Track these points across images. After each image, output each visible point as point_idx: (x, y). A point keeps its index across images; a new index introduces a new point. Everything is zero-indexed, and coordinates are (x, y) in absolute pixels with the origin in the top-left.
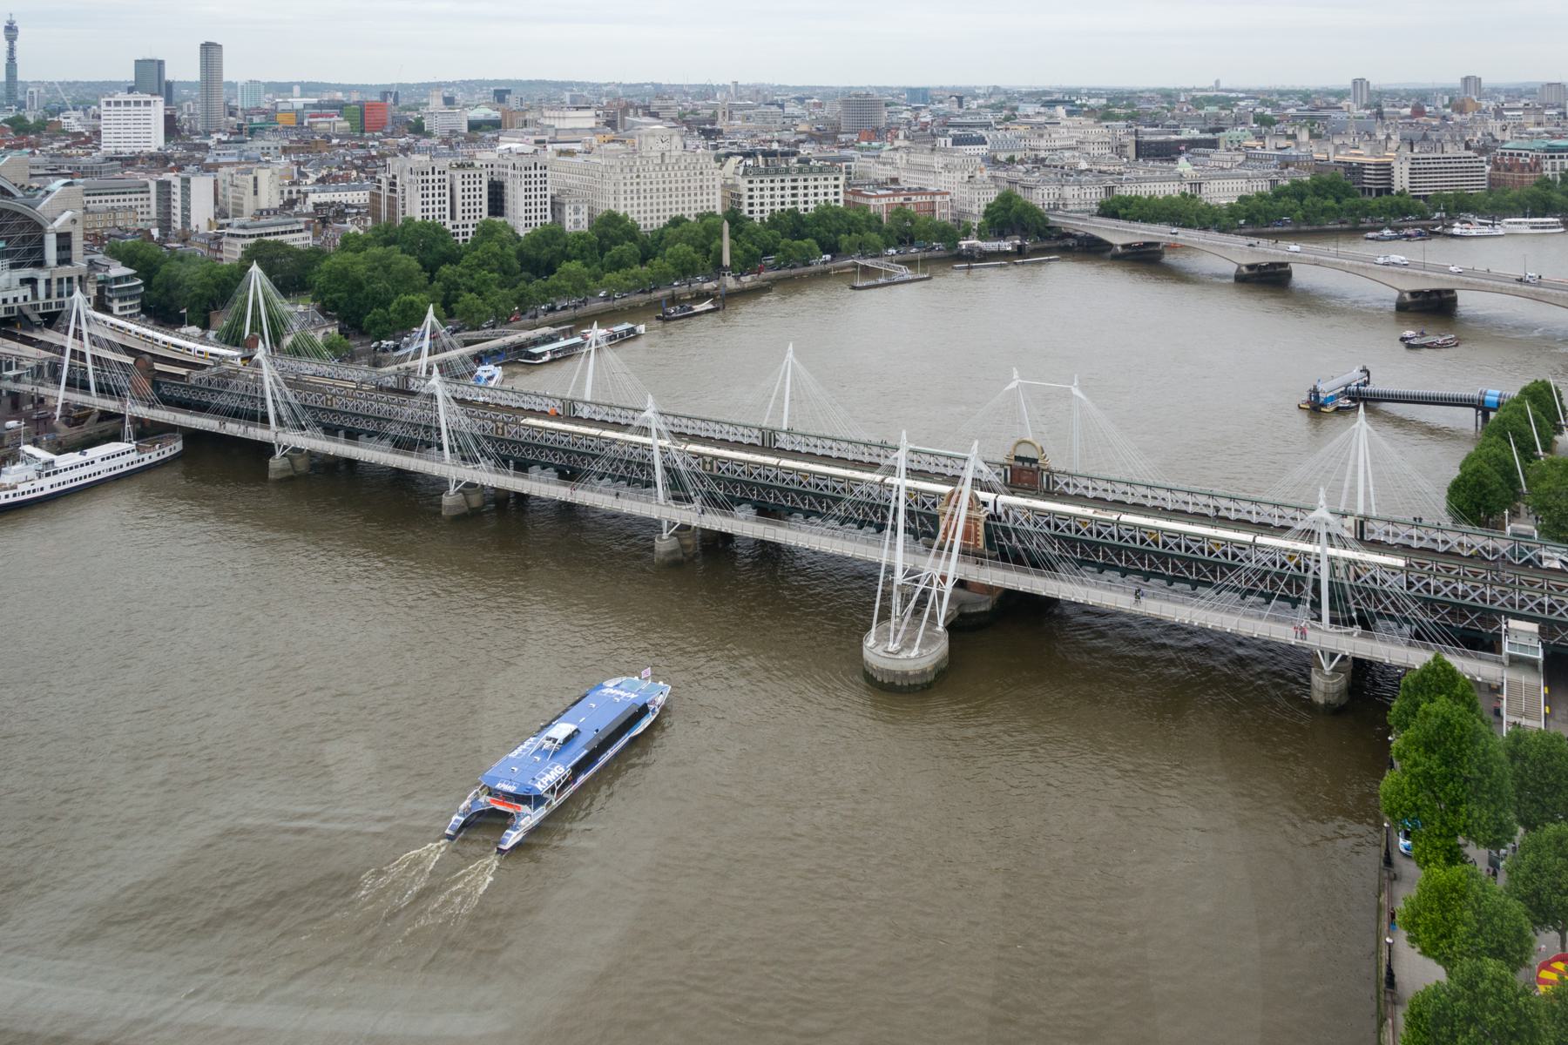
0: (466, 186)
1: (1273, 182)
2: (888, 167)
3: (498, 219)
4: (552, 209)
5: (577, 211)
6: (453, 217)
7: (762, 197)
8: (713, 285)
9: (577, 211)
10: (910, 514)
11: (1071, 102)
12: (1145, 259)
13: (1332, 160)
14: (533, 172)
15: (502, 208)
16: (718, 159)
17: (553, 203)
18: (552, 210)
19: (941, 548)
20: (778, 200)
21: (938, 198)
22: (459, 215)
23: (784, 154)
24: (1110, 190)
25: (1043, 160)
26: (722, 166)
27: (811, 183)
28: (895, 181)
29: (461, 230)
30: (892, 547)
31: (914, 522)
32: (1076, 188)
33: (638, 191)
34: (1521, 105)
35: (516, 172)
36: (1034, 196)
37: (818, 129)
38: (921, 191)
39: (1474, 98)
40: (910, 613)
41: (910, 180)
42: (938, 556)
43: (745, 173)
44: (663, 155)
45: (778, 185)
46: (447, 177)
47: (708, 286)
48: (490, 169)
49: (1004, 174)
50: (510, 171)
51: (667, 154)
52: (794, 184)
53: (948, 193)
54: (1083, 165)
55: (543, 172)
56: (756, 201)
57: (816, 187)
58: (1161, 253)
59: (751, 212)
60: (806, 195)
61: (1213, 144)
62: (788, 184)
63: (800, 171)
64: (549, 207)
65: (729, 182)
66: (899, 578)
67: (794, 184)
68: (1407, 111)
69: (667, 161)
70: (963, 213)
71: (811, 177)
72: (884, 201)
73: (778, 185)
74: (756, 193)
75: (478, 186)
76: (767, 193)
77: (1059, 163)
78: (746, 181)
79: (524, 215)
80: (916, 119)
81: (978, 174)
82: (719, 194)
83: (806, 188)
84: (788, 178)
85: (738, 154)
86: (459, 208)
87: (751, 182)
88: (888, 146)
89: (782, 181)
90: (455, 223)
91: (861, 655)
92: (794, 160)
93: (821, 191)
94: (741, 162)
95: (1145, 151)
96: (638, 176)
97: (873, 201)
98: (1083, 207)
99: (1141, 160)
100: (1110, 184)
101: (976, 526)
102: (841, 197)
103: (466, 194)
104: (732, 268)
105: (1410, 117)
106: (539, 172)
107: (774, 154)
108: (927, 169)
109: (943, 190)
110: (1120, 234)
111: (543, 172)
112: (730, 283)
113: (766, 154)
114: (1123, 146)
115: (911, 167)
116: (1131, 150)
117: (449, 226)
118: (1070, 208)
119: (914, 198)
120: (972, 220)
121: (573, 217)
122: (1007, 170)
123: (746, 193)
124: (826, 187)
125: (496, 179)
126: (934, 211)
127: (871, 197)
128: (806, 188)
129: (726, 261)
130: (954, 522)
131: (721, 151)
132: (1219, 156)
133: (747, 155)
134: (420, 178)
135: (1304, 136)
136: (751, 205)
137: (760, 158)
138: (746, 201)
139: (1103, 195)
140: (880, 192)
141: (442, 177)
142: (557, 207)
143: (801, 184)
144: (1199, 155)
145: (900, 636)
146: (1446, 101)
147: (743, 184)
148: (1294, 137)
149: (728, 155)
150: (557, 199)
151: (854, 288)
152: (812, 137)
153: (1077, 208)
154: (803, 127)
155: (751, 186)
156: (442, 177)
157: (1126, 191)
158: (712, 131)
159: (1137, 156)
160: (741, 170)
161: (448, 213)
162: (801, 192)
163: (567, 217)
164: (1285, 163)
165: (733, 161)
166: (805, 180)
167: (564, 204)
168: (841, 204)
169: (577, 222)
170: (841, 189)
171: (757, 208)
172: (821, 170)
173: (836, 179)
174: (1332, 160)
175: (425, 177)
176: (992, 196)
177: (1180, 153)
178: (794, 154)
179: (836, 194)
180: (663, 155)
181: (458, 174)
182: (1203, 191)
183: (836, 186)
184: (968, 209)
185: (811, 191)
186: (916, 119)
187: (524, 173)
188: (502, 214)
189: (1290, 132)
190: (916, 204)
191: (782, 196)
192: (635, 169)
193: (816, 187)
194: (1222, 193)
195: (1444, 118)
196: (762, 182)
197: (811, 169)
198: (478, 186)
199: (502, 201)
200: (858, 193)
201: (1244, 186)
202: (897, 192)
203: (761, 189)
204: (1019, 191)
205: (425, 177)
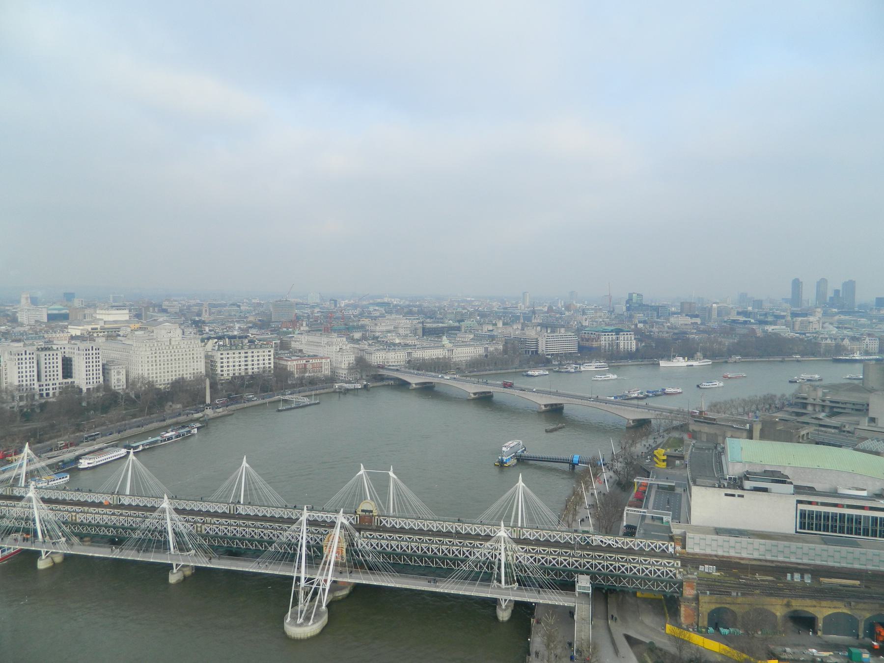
0: (48, 361)
1: (486, 349)
2: (297, 343)
3: (69, 380)
4: (103, 372)
5: (119, 373)
6: (39, 380)
7: (228, 362)
8: (200, 415)
9: (119, 373)
10: (309, 547)
11: (390, 309)
12: (427, 390)
13: (512, 337)
14: (91, 352)
15: (71, 373)
16: (202, 341)
17: (103, 369)
18: (103, 373)
19: (325, 564)
20: (237, 364)
21: (324, 361)
22: (43, 378)
23: (240, 337)
24: (409, 354)
25: (377, 338)
26: (206, 344)
27: (255, 354)
28: (301, 351)
29: (44, 387)
30: (299, 568)
31: (310, 551)
32: (393, 353)
33: (156, 361)
34: (593, 307)
35: (80, 352)
36: (373, 358)
37: (260, 320)
38: (315, 357)
39: (574, 302)
40: (308, 601)
41: (308, 350)
42: (323, 569)
43: (219, 350)
44: (170, 340)
45: (237, 355)
46: (34, 356)
47: (196, 416)
48: (63, 350)
49: (357, 346)
50: (76, 352)
51: (173, 339)
52: (246, 355)
54: (397, 341)
55: (97, 352)
56: (225, 364)
57: (258, 356)
58: (434, 387)
59: (222, 371)
60: (253, 361)
61: (458, 329)
62: (243, 355)
63: (250, 348)
64: (101, 372)
65: (210, 353)
66: (303, 583)
67: (246, 355)
68: (546, 309)
69: (173, 343)
70: (336, 368)
71: (255, 351)
72: (295, 363)
73: (237, 355)
74: (225, 360)
75: (55, 361)
76: (231, 360)
77: (385, 340)
78: (219, 353)
79: (85, 377)
80: (312, 314)
81: (344, 347)
82: (203, 361)
83: (253, 357)
84: (242, 351)
85: (215, 338)
86: (43, 374)
87: (222, 354)
88: (297, 332)
89: (240, 353)
90: (41, 383)
91: (283, 628)
92: (246, 341)
93: (261, 358)
94: (216, 343)
95: (427, 332)
96: (155, 353)
97: (289, 363)
98: (396, 364)
99: (425, 337)
100: (410, 351)
101: (342, 551)
102: (272, 361)
103: (48, 365)
105: (547, 312)
106: (94, 352)
107: (234, 337)
108: (318, 345)
109: (326, 355)
111: (97, 352)
112: (209, 412)
113: (230, 338)
114: (416, 329)
115: (309, 343)
116: (420, 332)
117: (36, 386)
118: (391, 364)
119: (311, 361)
120: (341, 371)
121: (116, 377)
122: (359, 344)
123: (219, 361)
124: (264, 356)
125: (67, 356)
126: (321, 367)
127: (288, 361)
128: (253, 357)
129: (208, 401)
130: (331, 550)
131: (205, 336)
132: (460, 337)
133: (220, 338)
134: (17, 357)
136: (222, 367)
137: (227, 339)
138: (219, 365)
139: (406, 357)
140: (293, 358)
141: (31, 356)
142: (105, 371)
143: (250, 354)
144: (452, 334)
145: (303, 615)
146: (562, 304)
147: (218, 356)
149: (209, 339)
150: (106, 367)
151: (279, 411)
152: (255, 326)
153: (393, 364)
154: (251, 319)
155: (222, 356)
156: (31, 356)
158: (199, 321)
159: (423, 336)
161: (36, 378)
162: (250, 359)
163: (113, 377)
164: (492, 338)
165: (211, 343)
166: (252, 352)
167: (110, 370)
168: (272, 366)
169: (119, 380)
170: (272, 356)
171: (225, 369)
172: (261, 347)
173: (269, 351)
174: (512, 337)
175: (20, 357)
176: (352, 359)
177: (443, 334)
178: (246, 337)
179: (269, 359)
180: (170, 340)
181: (42, 354)
182: (454, 354)
183: (269, 356)
184: (339, 366)
185: (256, 358)
186: (312, 314)
187: (85, 352)
188: (71, 377)
189: (494, 322)
190: (313, 364)
191: (240, 362)
192: (153, 349)
193: (258, 356)
194: (464, 353)
195: (561, 314)
196: (228, 354)
197: (255, 346)
198: (55, 361)
199: (71, 369)
200: (281, 359)
201: (473, 350)
202: (302, 358)
203: (228, 358)
204: (367, 357)
205: (20, 357)
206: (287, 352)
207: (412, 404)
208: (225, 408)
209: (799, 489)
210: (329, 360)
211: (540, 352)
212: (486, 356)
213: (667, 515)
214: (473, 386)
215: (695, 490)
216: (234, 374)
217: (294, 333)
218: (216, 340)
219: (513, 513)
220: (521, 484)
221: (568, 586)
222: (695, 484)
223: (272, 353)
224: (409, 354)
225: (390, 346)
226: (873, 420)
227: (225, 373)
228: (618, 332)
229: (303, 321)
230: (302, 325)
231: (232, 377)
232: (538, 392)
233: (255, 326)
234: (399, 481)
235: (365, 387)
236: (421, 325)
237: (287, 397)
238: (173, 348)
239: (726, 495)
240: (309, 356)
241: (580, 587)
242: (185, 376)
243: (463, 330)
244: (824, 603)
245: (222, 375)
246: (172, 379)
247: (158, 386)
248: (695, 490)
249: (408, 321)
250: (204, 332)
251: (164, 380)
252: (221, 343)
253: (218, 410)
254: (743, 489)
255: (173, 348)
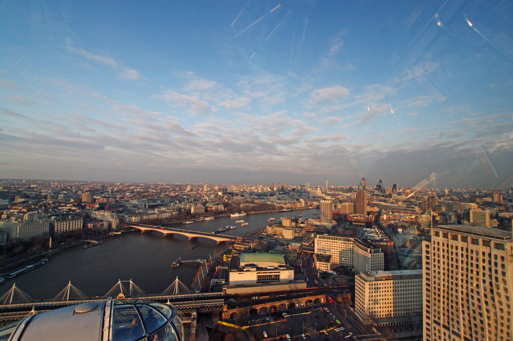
1: (172, 213)
53: (108, 221)
54: (137, 212)
61: (162, 205)
63: (72, 220)
72: (92, 224)
84: (68, 222)
100: (142, 216)
102: (82, 225)
104: (52, 248)
110: (143, 229)
118: (134, 222)
135: (178, 202)
137: (61, 216)
138: (56, 228)
148: (176, 202)
157: (145, 217)
160: (55, 221)
168: (82, 226)
170: (82, 223)
189: (176, 202)
206: (88, 219)
207: (142, 240)
208: (58, 248)
209: (259, 269)
210: (108, 222)
211: (192, 213)
212: (172, 216)
213: (223, 280)
214: (166, 231)
215: (230, 273)
216: (63, 231)
217: (92, 210)
218: (55, 217)
219: (174, 290)
220: (177, 280)
221: (189, 315)
222: (231, 272)
223: (82, 221)
224: (142, 217)
225: (134, 214)
226: (283, 236)
227: (59, 231)
228: (218, 204)
229: (97, 203)
230: (96, 205)
231: (62, 233)
232: (189, 232)
233: (74, 206)
234: (134, 284)
235: (123, 233)
236: (147, 204)
237: (88, 241)
238: (34, 223)
239: (239, 274)
240: (99, 221)
241: (193, 315)
242: (39, 234)
243: (164, 205)
244: (259, 305)
245: (58, 232)
246: (32, 236)
247: (24, 240)
248: (230, 273)
249: (142, 202)
250: (49, 211)
251: (28, 237)
252: (58, 218)
253: (55, 250)
254: (244, 271)
255: (34, 223)
